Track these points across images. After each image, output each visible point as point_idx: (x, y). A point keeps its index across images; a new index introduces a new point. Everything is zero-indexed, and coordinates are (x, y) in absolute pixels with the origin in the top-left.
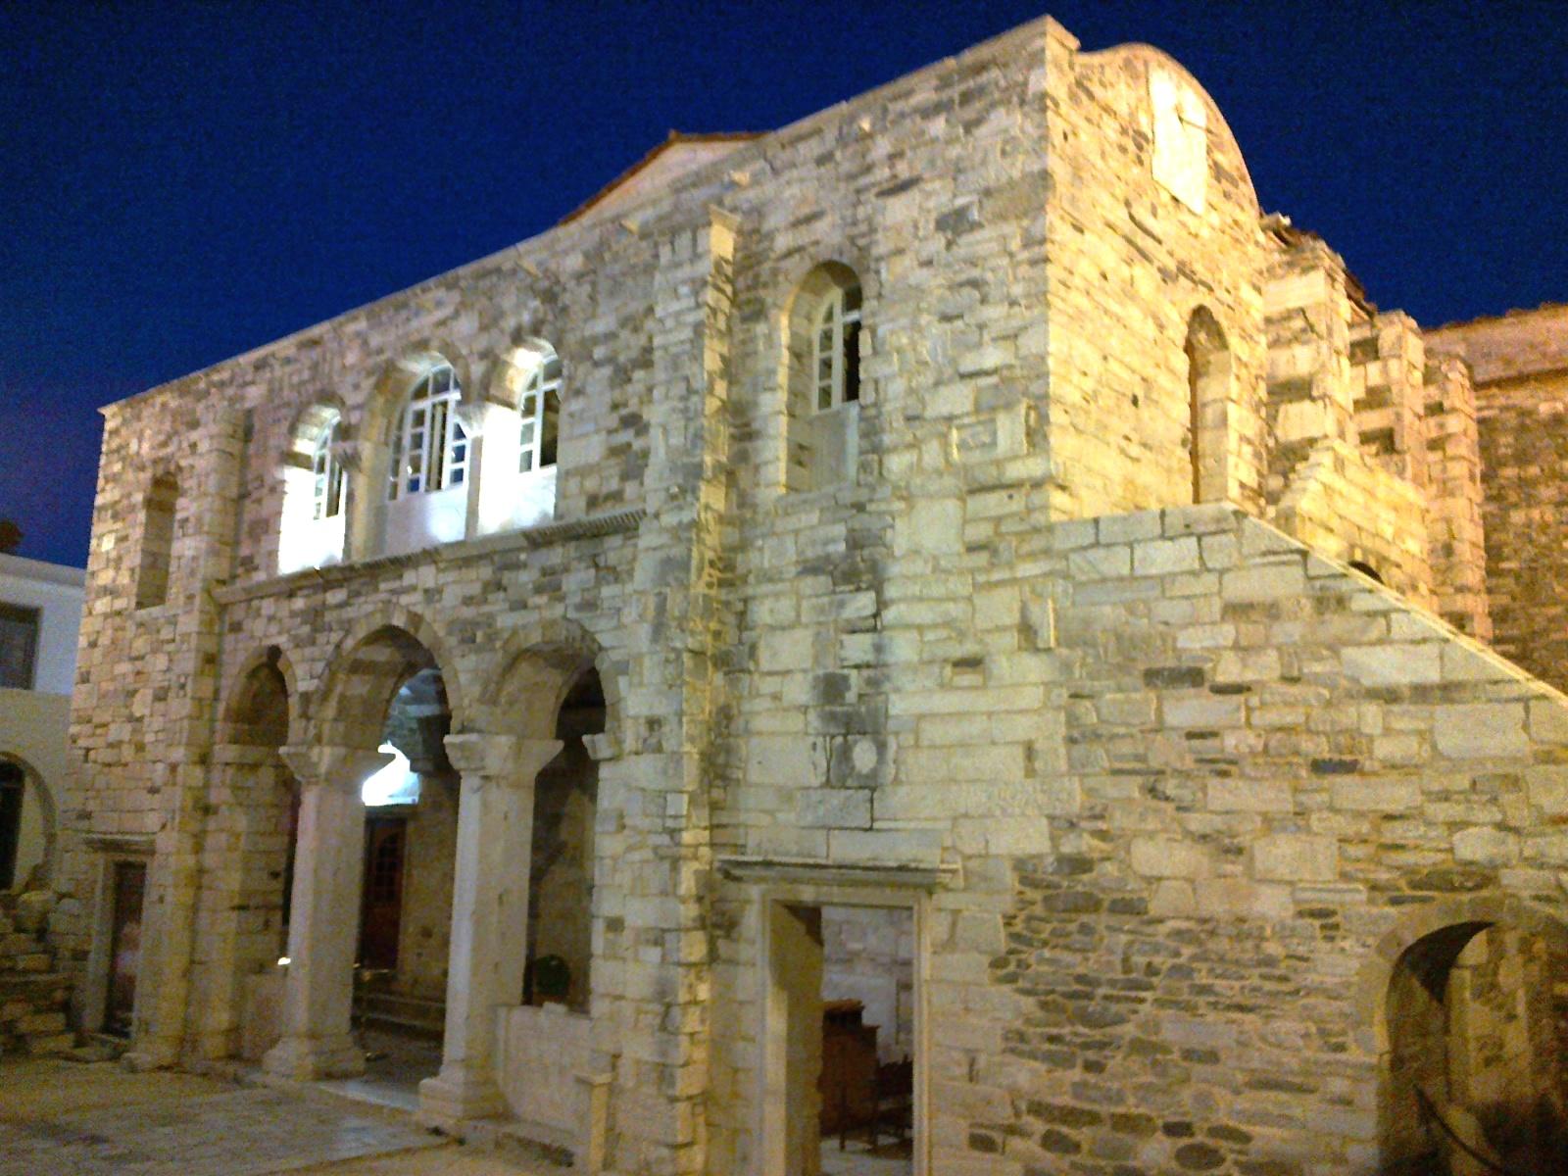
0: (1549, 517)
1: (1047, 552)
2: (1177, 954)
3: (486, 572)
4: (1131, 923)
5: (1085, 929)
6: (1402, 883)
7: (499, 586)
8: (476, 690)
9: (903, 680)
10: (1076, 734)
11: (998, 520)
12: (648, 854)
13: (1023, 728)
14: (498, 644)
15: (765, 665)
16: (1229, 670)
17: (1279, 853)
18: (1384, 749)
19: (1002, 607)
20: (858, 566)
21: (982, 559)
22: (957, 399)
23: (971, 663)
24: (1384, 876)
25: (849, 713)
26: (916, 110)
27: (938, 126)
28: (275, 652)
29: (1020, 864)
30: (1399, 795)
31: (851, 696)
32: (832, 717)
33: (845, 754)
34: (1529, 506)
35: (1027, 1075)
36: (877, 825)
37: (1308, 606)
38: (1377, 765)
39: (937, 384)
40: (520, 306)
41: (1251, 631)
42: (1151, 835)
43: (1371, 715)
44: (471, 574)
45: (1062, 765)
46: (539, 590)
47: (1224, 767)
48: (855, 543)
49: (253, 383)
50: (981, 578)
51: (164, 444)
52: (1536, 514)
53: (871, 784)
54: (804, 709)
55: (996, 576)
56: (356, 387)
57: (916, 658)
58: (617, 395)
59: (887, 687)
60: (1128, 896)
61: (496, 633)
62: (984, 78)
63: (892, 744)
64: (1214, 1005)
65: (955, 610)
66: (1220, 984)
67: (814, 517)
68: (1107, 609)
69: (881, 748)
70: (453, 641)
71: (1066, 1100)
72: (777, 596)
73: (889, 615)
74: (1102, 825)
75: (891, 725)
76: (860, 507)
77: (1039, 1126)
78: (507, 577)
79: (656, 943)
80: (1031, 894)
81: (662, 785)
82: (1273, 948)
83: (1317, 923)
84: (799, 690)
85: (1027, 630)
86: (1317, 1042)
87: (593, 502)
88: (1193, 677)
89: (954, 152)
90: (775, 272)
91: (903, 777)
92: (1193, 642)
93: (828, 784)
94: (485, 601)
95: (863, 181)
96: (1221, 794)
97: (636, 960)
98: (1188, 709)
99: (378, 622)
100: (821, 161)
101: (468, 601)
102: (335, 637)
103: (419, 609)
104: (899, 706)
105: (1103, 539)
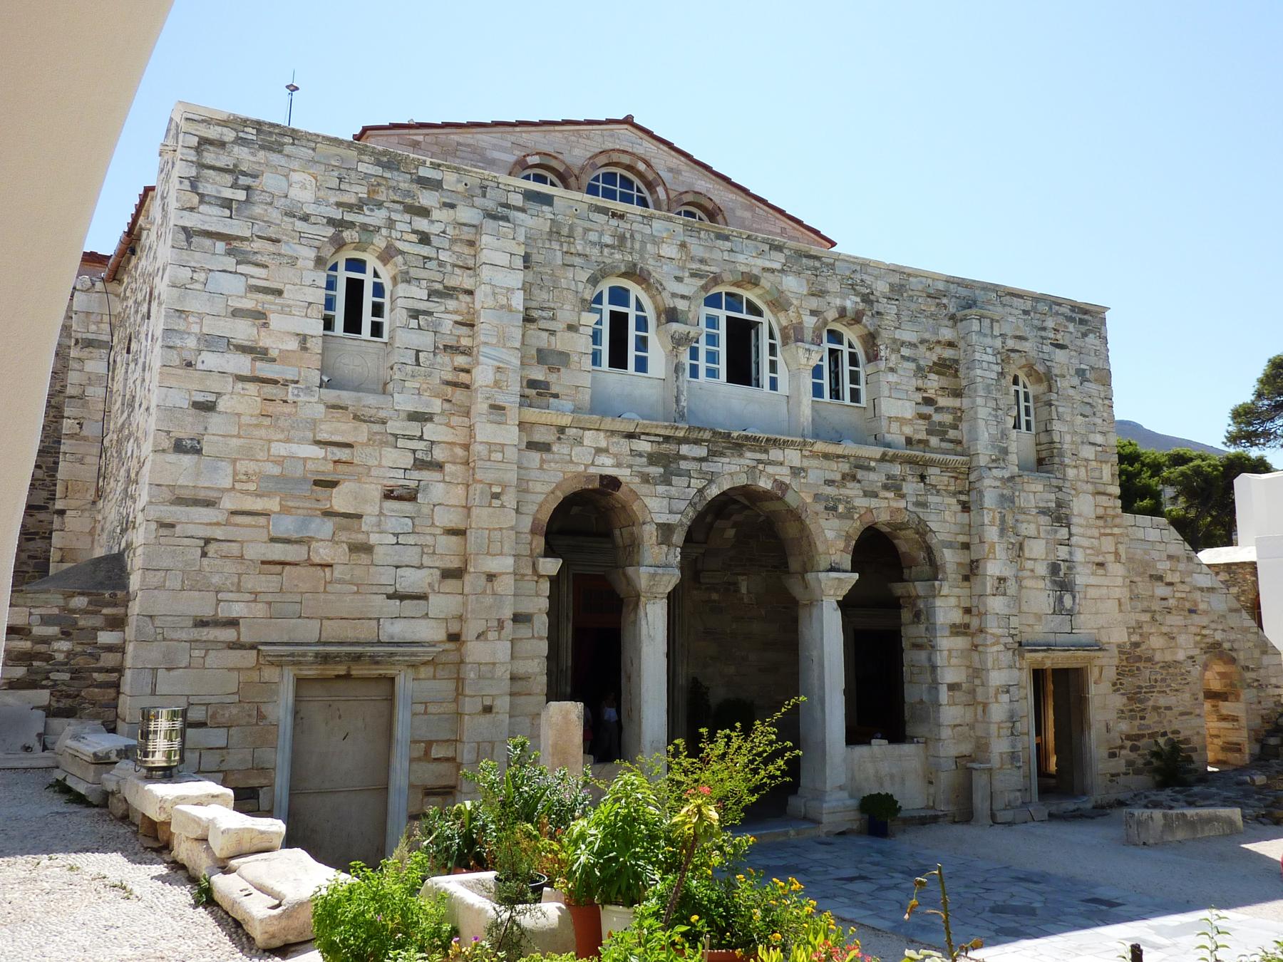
3: (845, 467)
5: (1138, 669)
7: (854, 478)
8: (841, 545)
9: (1079, 569)
11: (1106, 508)
12: (1001, 647)
14: (856, 516)
15: (1027, 555)
16: (1169, 579)
19: (1108, 544)
20: (1059, 516)
21: (1101, 523)
22: (1088, 452)
23: (1101, 565)
25: (1061, 580)
26: (1062, 314)
27: (1071, 327)
28: (612, 483)
29: (1119, 646)
31: (1062, 574)
32: (1054, 582)
33: (1061, 599)
35: (1124, 726)
40: (844, 297)
43: (1197, 595)
44: (834, 466)
46: (886, 487)
48: (1060, 504)
49: (523, 210)
51: (358, 207)
53: (1071, 613)
54: (1044, 578)
56: (679, 279)
58: (920, 383)
59: (1074, 571)
61: (854, 508)
62: (1086, 317)
67: (1040, 488)
69: (1074, 597)
70: (820, 507)
71: (1136, 732)
72: (1029, 522)
73: (1074, 539)
75: (1077, 588)
76: (1060, 489)
77: (1128, 744)
78: (860, 474)
79: (1008, 692)
80: (1124, 657)
81: (1006, 611)
84: (1042, 569)
85: (1117, 554)
87: (909, 441)
88: (1160, 578)
89: (1079, 342)
90: (1009, 357)
93: (1054, 613)
94: (844, 487)
95: (1043, 334)
97: (997, 701)
98: (1161, 590)
99: (742, 480)
100: (1026, 312)
101: (829, 482)
102: (697, 483)
103: (787, 480)
104: (1080, 580)
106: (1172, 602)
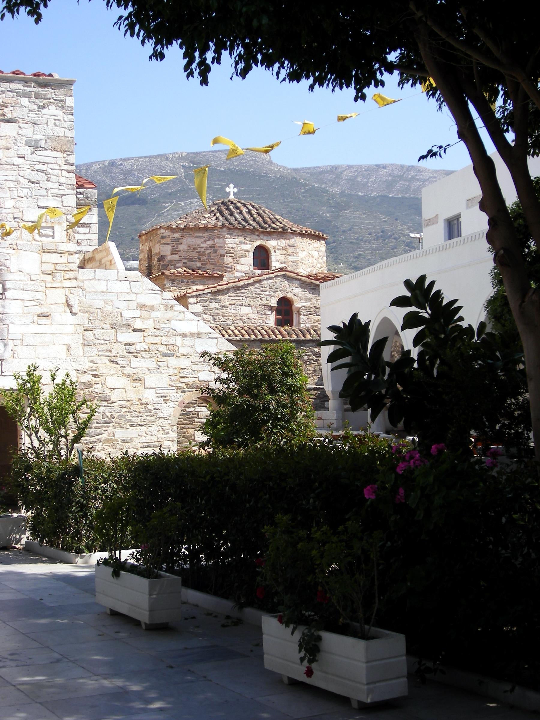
1: (75, 279)
2: (121, 411)
4: (106, 404)
6: (185, 387)
10: (86, 342)
13: (67, 340)
16: (138, 325)
17: (151, 380)
18: (182, 350)
21: (49, 278)
23: (46, 316)
24: (180, 385)
27: (25, 101)
30: (185, 362)
36: (3, 374)
37: (162, 307)
38: (180, 355)
39: (29, 207)
41: (145, 314)
42: (112, 375)
43: (179, 341)
45: (81, 353)
47: (135, 354)
50: (49, 285)
55: (54, 285)
57: (21, 312)
60: (105, 395)
63: (10, 343)
64: (132, 426)
65: (39, 295)
66: (134, 419)
68: (98, 301)
73: (8, 294)
74: (95, 373)
82: (150, 407)
83: (162, 399)
86: (161, 432)
91: (15, 356)
92: (127, 314)
96: (135, 362)
98: (126, 336)
105: (97, 278)
106: (139, 347)
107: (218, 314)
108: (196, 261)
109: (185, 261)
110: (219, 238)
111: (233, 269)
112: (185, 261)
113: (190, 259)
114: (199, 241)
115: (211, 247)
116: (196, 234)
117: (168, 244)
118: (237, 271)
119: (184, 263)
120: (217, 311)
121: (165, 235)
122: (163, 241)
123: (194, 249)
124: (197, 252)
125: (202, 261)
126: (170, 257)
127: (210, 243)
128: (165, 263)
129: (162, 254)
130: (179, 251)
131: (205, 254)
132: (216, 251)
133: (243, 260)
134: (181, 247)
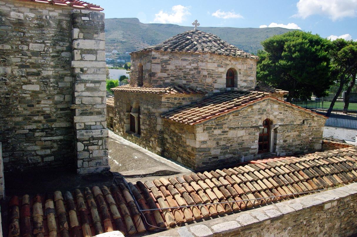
0: (16, 72)
34: (5, 65)
52: (9, 70)
107: (220, 139)
108: (182, 79)
109: (173, 78)
110: (202, 61)
111: (212, 87)
112: (173, 78)
113: (177, 77)
114: (185, 63)
115: (195, 69)
116: (183, 58)
117: (158, 64)
118: (215, 89)
119: (172, 80)
120: (220, 137)
121: (155, 56)
122: (153, 61)
123: (180, 69)
124: (182, 72)
125: (188, 80)
126: (160, 75)
127: (194, 65)
128: (155, 79)
129: (153, 71)
130: (168, 70)
131: (190, 74)
132: (199, 72)
133: (219, 80)
134: (169, 67)
